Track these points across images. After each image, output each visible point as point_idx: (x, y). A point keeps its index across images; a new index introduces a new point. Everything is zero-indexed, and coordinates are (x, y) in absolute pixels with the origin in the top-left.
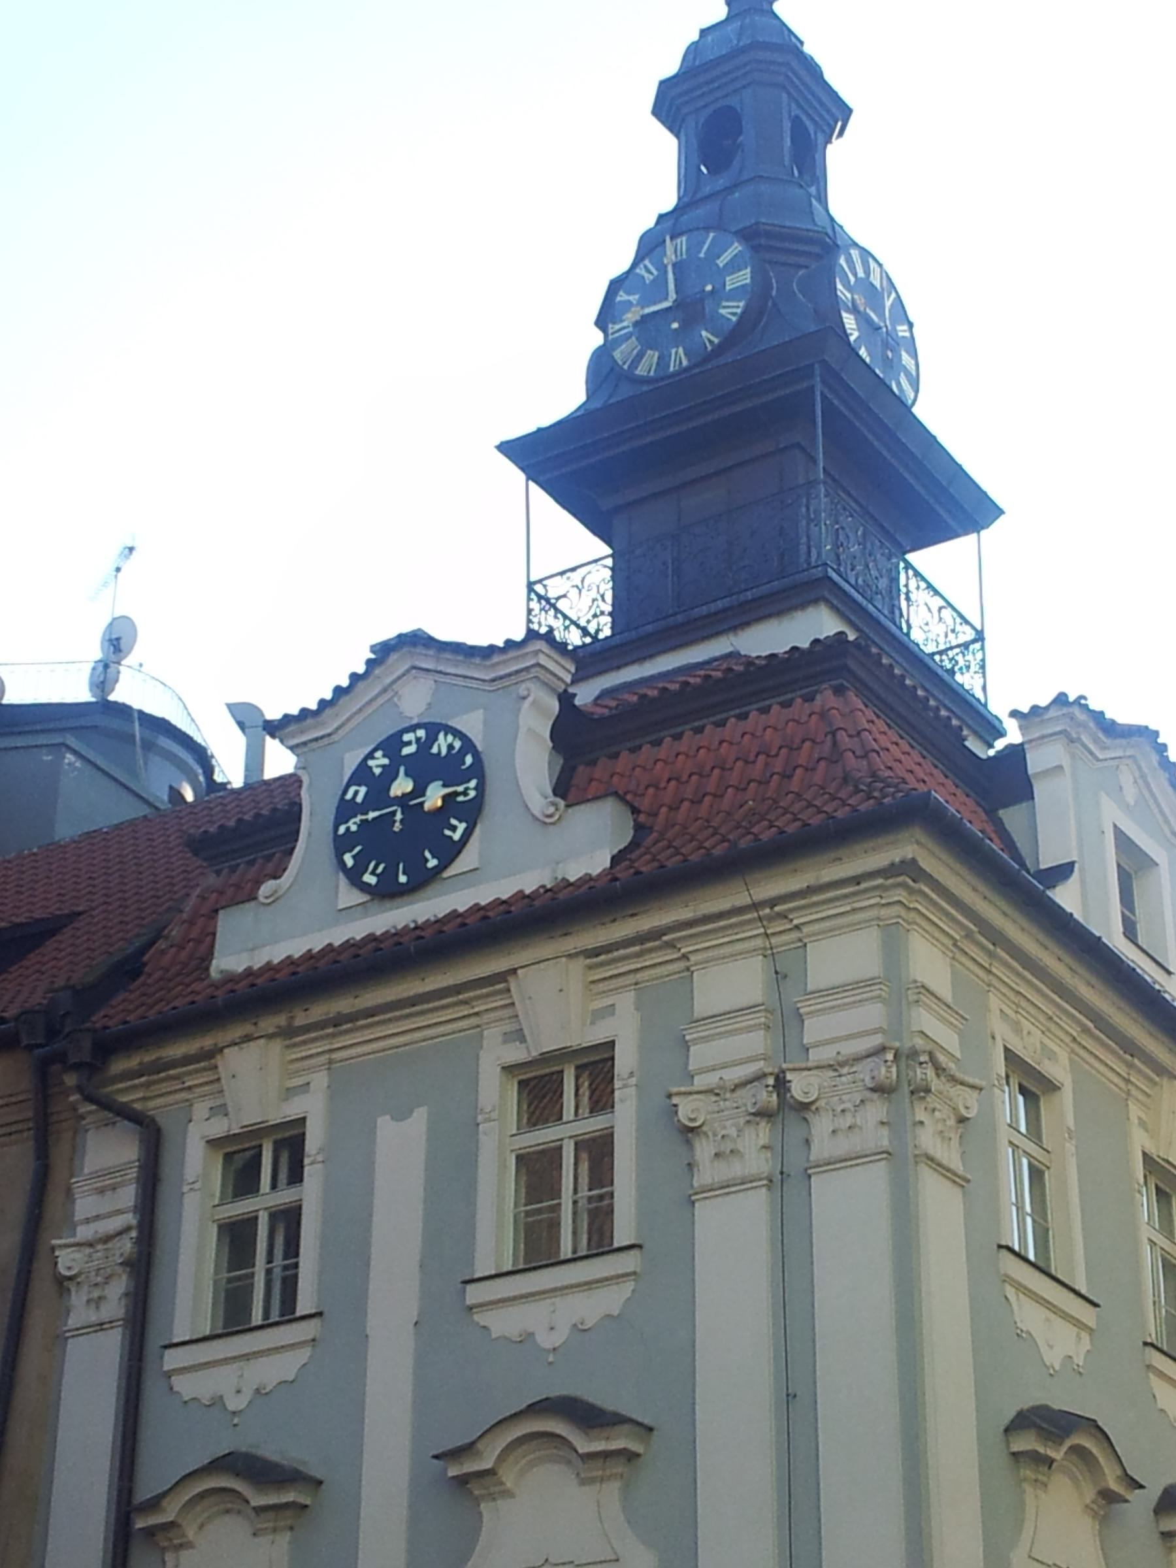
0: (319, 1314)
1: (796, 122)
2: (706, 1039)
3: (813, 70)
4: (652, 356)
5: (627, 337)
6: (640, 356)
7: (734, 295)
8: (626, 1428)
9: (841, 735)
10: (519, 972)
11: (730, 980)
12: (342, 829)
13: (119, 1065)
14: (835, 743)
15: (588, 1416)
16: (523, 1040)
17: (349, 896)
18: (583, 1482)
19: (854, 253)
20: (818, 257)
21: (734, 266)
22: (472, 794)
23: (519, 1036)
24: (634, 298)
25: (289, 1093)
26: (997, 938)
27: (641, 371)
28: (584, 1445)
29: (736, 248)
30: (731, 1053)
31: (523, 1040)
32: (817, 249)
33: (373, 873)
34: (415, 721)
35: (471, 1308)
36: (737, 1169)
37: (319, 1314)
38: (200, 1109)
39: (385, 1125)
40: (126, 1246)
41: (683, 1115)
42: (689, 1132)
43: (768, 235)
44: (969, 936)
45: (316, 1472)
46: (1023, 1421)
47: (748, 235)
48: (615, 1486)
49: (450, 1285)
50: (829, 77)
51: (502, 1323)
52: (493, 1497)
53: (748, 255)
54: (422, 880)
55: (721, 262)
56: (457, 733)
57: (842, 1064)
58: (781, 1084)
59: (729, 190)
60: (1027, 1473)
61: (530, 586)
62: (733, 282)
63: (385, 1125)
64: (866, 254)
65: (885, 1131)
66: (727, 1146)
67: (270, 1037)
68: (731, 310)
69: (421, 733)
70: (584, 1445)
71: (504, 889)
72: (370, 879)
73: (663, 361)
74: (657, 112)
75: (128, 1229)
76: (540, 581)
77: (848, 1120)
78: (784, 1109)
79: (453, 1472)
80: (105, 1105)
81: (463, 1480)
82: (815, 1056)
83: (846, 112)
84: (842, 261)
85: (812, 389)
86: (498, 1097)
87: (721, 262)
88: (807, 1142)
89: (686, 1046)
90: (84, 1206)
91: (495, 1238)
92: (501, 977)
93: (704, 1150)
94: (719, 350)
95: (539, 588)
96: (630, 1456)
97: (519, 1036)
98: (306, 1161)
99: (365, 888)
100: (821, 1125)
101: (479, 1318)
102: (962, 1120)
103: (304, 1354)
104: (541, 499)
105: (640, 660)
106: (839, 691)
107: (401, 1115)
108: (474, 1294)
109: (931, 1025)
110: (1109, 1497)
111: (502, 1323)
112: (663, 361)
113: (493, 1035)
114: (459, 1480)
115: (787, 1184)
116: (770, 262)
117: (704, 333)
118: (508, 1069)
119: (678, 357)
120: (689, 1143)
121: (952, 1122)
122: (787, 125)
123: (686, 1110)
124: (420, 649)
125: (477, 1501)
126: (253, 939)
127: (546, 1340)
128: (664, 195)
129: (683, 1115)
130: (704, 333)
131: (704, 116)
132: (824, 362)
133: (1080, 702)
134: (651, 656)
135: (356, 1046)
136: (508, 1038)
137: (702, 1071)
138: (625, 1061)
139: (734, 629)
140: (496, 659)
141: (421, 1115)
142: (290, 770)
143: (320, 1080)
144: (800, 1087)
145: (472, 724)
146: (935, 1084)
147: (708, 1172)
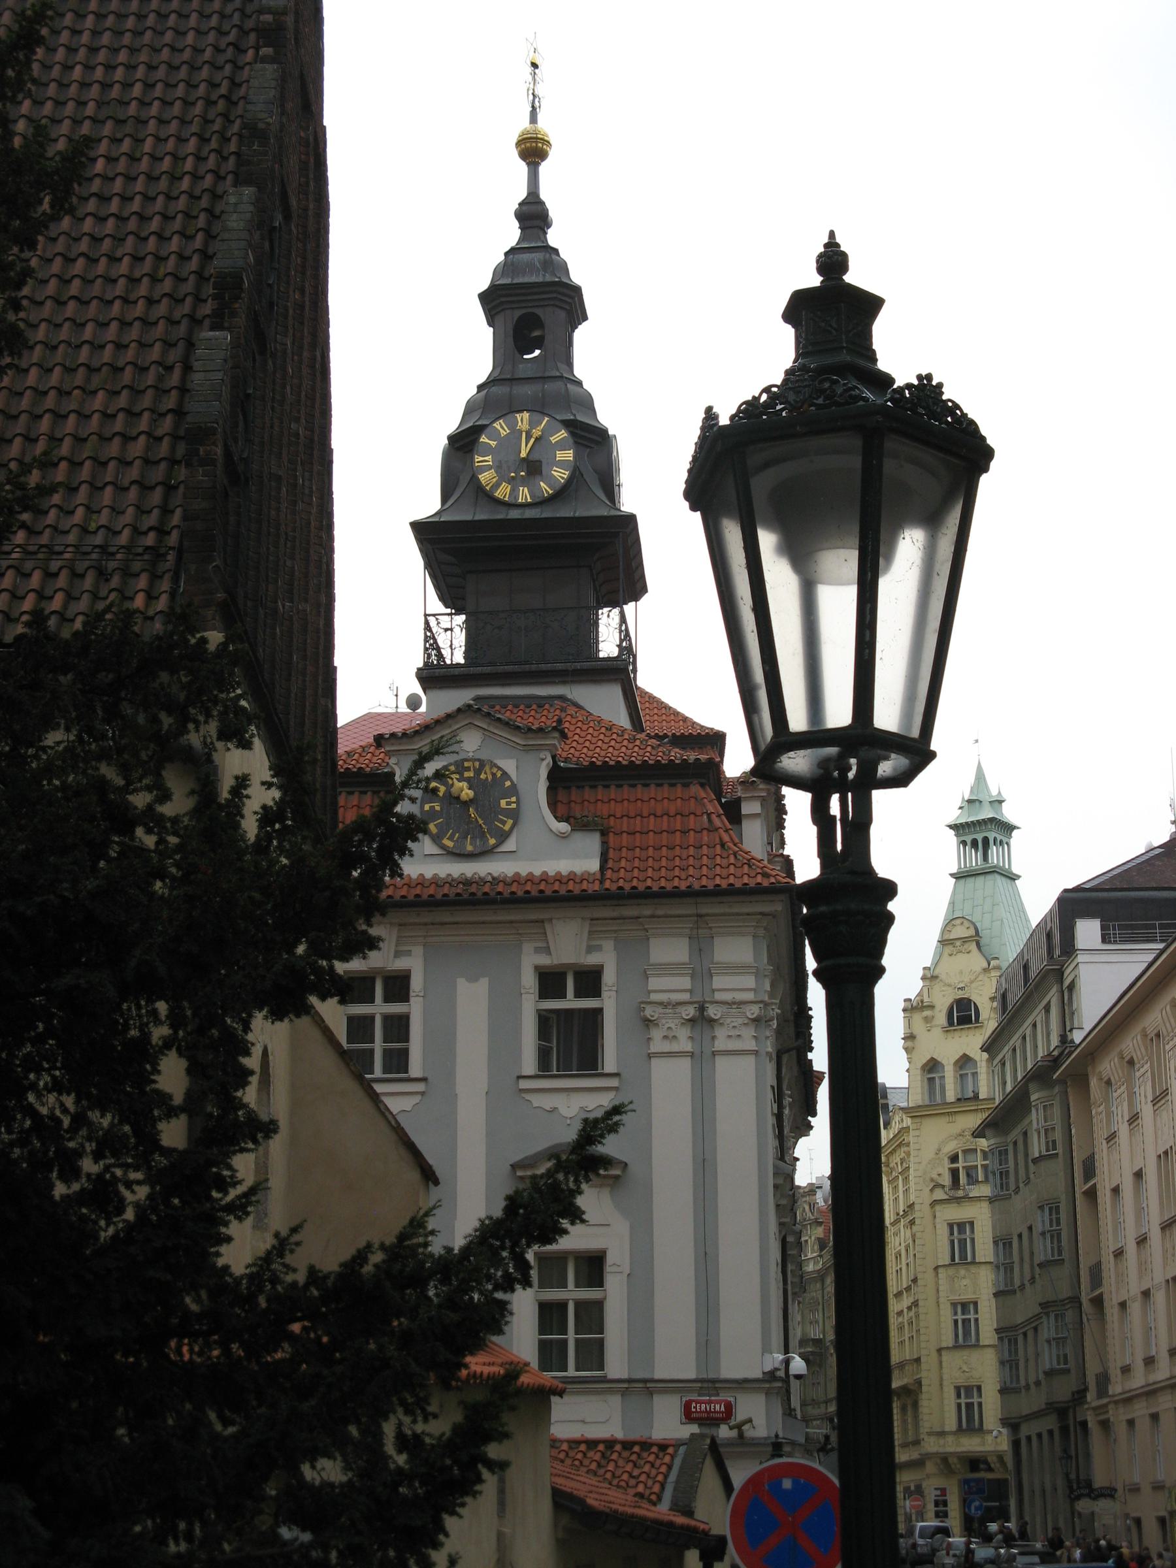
0: (424, 1080)
2: (659, 975)
5: (490, 467)
6: (497, 485)
7: (562, 464)
9: (714, 816)
10: (554, 921)
11: (670, 949)
12: (427, 807)
14: (710, 820)
16: (550, 953)
20: (597, 443)
21: (561, 445)
22: (514, 806)
23: (547, 950)
24: (493, 443)
27: (498, 494)
29: (563, 434)
30: (672, 986)
31: (550, 953)
33: (451, 838)
34: (471, 754)
36: (675, 1047)
37: (424, 1080)
39: (463, 986)
42: (648, 1023)
47: (567, 424)
53: (571, 441)
54: (485, 853)
55: (554, 439)
56: (500, 768)
57: (734, 1003)
58: (702, 1009)
59: (545, 379)
61: (426, 615)
63: (462, 983)
66: (671, 1034)
67: (391, 924)
68: (561, 475)
69: (477, 764)
71: (538, 869)
72: (447, 842)
73: (514, 491)
76: (434, 615)
78: (701, 1021)
79: (519, 1173)
82: (718, 996)
83: (585, 318)
86: (529, 981)
87: (554, 439)
88: (714, 1038)
89: (647, 977)
92: (542, 921)
93: (656, 1034)
95: (432, 620)
96: (617, 1177)
97: (547, 950)
98: (412, 994)
99: (443, 847)
100: (721, 1033)
103: (417, 1099)
105: (503, 685)
106: (702, 785)
107: (473, 979)
108: (524, 1084)
111: (538, 1100)
113: (528, 948)
115: (703, 1061)
117: (542, 484)
118: (537, 968)
119: (524, 495)
120: (647, 1026)
123: (649, 1012)
124: (478, 716)
130: (542, 484)
131: (518, 313)
134: (509, 685)
136: (537, 950)
137: (655, 991)
138: (609, 978)
139: (564, 683)
140: (530, 735)
141: (483, 985)
144: (712, 1011)
145: (509, 765)
147: (657, 1046)
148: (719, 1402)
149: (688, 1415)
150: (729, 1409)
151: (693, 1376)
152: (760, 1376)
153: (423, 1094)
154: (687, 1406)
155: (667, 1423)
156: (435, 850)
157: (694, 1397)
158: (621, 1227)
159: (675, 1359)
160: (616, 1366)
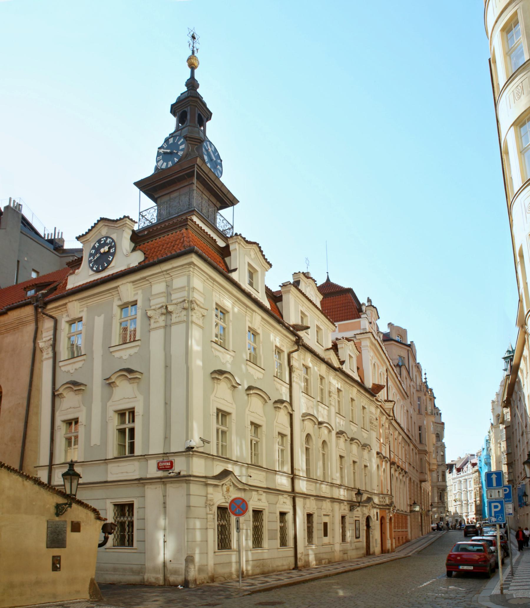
1: (199, 115)
3: (204, 104)
4: (165, 164)
7: (182, 150)
8: (137, 373)
13: (50, 307)
15: (130, 371)
17: (91, 272)
18: (130, 383)
19: (208, 143)
21: (181, 144)
25: (80, 312)
26: (214, 280)
28: (130, 376)
32: (199, 141)
35: (111, 352)
38: (64, 316)
40: (51, 342)
41: (148, 314)
43: (189, 137)
44: (207, 279)
45: (85, 383)
46: (215, 372)
47: (185, 138)
48: (136, 384)
49: (108, 348)
50: (208, 106)
51: (117, 355)
52: (115, 387)
55: (179, 143)
60: (216, 381)
62: (181, 147)
64: (211, 143)
65: (185, 317)
68: (180, 153)
70: (130, 376)
74: (171, 112)
75: (51, 339)
77: (179, 315)
79: (107, 382)
80: (47, 315)
81: (109, 384)
84: (205, 144)
85: (194, 171)
87: (179, 143)
90: (44, 334)
91: (116, 339)
94: (178, 162)
101: (113, 354)
102: (203, 316)
104: (141, 192)
108: (112, 349)
109: (197, 296)
110: (234, 387)
111: (117, 355)
112: (167, 165)
114: (109, 384)
116: (190, 144)
119: (170, 164)
121: (201, 316)
122: (197, 115)
125: (112, 387)
126: (74, 281)
127: (124, 358)
128: (172, 129)
129: (148, 314)
132: (197, 164)
133: (240, 234)
135: (92, 302)
137: (153, 305)
142: (81, 247)
143: (85, 309)
146: (196, 308)
148: (168, 462)
149: (159, 468)
150: (172, 463)
151: (162, 452)
152: (184, 450)
153: (84, 360)
154: (158, 464)
155: (152, 471)
156: (93, 273)
157: (161, 459)
158: (141, 398)
159: (156, 448)
160: (138, 451)
